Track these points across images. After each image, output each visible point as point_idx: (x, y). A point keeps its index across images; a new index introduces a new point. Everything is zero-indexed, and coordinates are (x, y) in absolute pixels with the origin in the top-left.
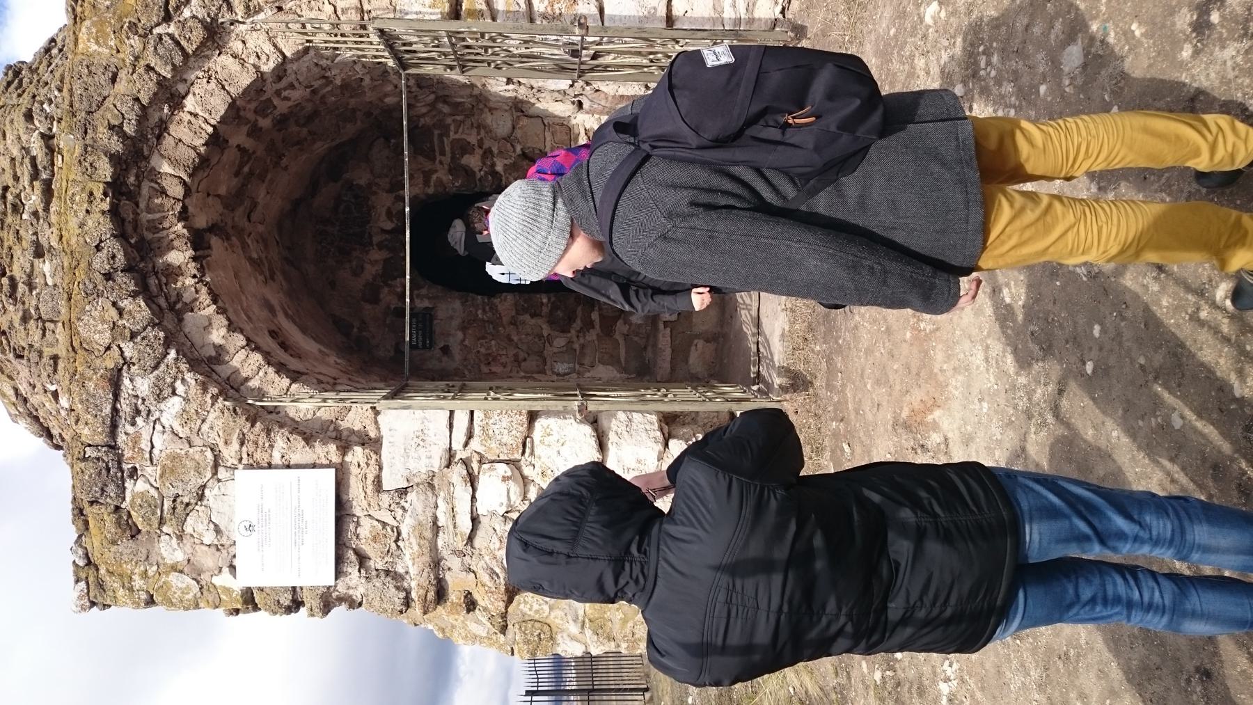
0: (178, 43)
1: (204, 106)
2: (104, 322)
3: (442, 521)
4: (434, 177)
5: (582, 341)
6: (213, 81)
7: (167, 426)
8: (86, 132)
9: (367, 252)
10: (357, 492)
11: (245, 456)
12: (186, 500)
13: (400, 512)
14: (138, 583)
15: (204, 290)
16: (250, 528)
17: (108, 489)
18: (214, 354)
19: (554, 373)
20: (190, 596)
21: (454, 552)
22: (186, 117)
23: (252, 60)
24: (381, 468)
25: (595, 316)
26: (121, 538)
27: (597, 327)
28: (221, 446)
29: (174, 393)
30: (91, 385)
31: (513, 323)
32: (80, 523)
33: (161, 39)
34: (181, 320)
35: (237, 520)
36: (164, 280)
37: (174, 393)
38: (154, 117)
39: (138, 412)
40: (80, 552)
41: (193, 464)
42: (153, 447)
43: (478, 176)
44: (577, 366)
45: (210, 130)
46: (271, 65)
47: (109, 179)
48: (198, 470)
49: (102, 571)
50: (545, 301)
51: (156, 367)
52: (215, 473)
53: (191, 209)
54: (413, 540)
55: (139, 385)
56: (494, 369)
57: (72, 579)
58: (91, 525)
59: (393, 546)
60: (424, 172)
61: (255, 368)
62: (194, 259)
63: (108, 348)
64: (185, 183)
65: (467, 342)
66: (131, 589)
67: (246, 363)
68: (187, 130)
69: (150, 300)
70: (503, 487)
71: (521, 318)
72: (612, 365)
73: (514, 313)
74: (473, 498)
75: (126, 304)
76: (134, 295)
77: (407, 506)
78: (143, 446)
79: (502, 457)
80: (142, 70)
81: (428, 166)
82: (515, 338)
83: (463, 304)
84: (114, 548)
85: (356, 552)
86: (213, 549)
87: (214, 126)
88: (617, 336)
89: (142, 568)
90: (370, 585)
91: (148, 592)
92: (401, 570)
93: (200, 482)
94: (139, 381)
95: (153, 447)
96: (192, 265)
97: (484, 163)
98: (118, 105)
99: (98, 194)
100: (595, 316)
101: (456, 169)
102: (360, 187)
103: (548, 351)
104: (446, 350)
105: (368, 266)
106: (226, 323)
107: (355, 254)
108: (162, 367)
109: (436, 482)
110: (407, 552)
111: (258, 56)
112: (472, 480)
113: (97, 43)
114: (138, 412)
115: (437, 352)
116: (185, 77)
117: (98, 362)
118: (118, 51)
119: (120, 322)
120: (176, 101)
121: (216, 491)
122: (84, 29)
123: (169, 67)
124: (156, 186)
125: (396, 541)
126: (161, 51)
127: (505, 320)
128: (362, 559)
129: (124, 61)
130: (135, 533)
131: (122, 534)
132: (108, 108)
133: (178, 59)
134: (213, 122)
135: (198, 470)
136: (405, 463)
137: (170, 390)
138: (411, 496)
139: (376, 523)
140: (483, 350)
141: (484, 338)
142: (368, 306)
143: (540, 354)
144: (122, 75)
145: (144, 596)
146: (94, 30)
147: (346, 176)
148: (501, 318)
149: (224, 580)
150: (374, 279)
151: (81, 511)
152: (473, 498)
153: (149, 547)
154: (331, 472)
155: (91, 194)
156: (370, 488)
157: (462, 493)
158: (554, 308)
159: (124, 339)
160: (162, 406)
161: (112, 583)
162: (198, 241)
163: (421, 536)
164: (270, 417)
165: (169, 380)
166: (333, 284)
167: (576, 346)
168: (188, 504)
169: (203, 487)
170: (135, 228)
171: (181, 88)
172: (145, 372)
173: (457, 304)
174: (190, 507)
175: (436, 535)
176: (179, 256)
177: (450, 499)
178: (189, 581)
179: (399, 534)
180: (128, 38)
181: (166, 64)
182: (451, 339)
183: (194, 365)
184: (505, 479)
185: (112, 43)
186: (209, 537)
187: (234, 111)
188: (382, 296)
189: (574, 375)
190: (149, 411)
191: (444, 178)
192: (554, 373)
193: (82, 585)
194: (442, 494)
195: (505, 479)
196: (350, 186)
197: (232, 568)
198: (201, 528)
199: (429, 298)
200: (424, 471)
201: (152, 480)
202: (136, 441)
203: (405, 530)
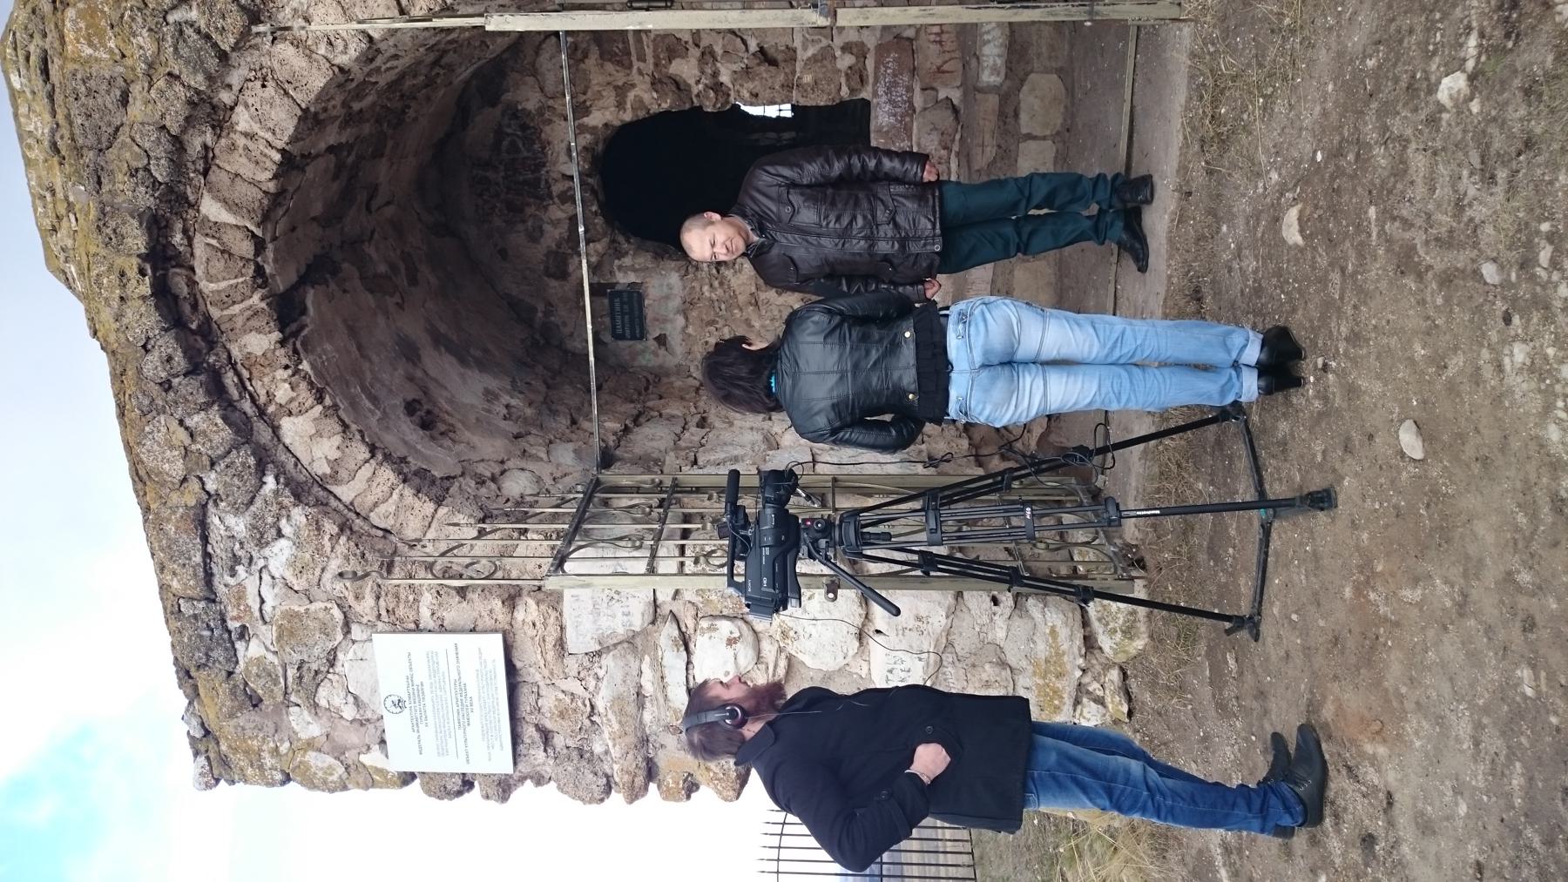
0: (208, 37)
1: (263, 124)
2: (172, 448)
4: (631, 95)
6: (270, 84)
7: (277, 575)
8: (99, 183)
9: (546, 208)
10: (531, 658)
11: (384, 613)
12: (314, 667)
13: (592, 683)
14: (268, 761)
15: (303, 385)
16: (399, 704)
17: (214, 654)
18: (328, 471)
20: (335, 778)
22: (241, 142)
23: (322, 49)
24: (562, 628)
26: (240, 708)
28: (351, 600)
29: (280, 534)
30: (170, 528)
32: (189, 691)
33: (181, 32)
34: (275, 430)
35: (384, 691)
36: (246, 374)
37: (280, 534)
38: (195, 143)
39: (236, 560)
40: (195, 722)
41: (316, 624)
42: (263, 602)
43: (695, 91)
45: (277, 157)
46: (353, 53)
47: (143, 251)
48: (326, 631)
49: (224, 748)
51: (251, 502)
52: (347, 630)
53: (268, 270)
54: (611, 716)
55: (229, 524)
57: (190, 752)
58: (201, 691)
59: (587, 722)
60: (616, 88)
61: (386, 489)
62: (282, 343)
63: (185, 480)
64: (254, 235)
65: (690, 330)
66: (261, 767)
67: (370, 487)
68: (244, 160)
69: (228, 407)
70: (730, 652)
71: (763, 296)
73: (753, 289)
75: (195, 421)
76: (204, 407)
77: (601, 673)
78: (250, 602)
79: (725, 612)
80: (161, 83)
82: (757, 325)
83: (682, 278)
84: (233, 722)
86: (356, 725)
87: (283, 151)
89: (272, 745)
90: (560, 769)
91: (283, 771)
92: (598, 749)
93: (330, 646)
94: (231, 520)
95: (263, 602)
96: (281, 352)
98: (137, 138)
99: (132, 273)
104: (662, 340)
105: (547, 227)
106: (339, 429)
107: (530, 210)
108: (259, 502)
109: (638, 641)
110: (606, 731)
111: (331, 44)
112: (685, 642)
113: (91, 44)
114: (236, 560)
116: (228, 80)
117: (175, 497)
118: (124, 56)
119: (194, 447)
120: (219, 119)
121: (350, 655)
122: (68, 24)
123: (200, 77)
124: (214, 242)
125: (589, 717)
126: (184, 52)
127: (742, 299)
128: (546, 736)
129: (133, 69)
130: (256, 702)
131: (243, 703)
132: (124, 144)
133: (212, 63)
134: (280, 144)
135: (326, 631)
136: (595, 622)
137: (273, 531)
138: (607, 660)
139: (561, 696)
141: (712, 323)
142: (554, 283)
144: (136, 89)
145: (279, 777)
146: (82, 25)
147: (508, 97)
148: (735, 296)
149: (372, 759)
150: (559, 246)
151: (188, 673)
152: (689, 663)
153: (276, 719)
154: (499, 637)
155: (122, 274)
156: (551, 655)
157: (674, 661)
159: (204, 468)
160: (266, 552)
161: (239, 760)
162: (286, 313)
163: (621, 712)
164: (412, 553)
165: (270, 520)
166: (503, 253)
168: (317, 672)
169: (335, 650)
170: (195, 307)
171: (226, 97)
172: (237, 511)
173: (674, 278)
174: (321, 676)
175: (641, 706)
176: (258, 342)
177: (658, 665)
178: (330, 760)
179: (593, 707)
180: (135, 35)
181: (195, 71)
182: (669, 326)
183: (299, 496)
184: (731, 642)
185: (112, 44)
186: (349, 712)
187: (310, 120)
190: (251, 558)
193: (202, 760)
194: (647, 658)
195: (731, 642)
196: (514, 112)
197: (383, 742)
198: (337, 701)
199: (635, 270)
200: (621, 631)
201: (268, 643)
202: (240, 594)
203: (601, 705)
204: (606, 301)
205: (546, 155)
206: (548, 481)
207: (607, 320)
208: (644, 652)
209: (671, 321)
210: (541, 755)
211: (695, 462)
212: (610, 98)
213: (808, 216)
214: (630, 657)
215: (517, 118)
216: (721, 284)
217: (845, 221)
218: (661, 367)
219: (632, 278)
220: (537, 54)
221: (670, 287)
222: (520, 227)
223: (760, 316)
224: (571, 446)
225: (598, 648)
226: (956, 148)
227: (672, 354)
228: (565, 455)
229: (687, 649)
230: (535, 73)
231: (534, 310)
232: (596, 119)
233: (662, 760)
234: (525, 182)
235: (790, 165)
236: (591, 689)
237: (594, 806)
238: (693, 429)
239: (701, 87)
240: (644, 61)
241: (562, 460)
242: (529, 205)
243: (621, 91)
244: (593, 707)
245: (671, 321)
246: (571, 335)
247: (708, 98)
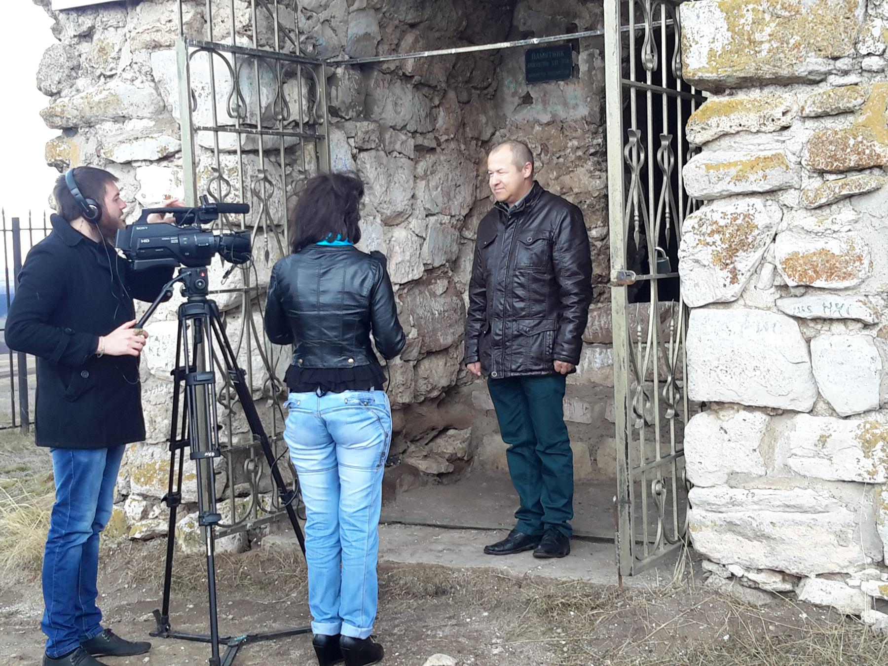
3: (129, 126)
13: (128, 75)
21: (100, 145)
54: (105, 93)
59: (98, 73)
65: (537, 128)
74: (151, 162)
77: (137, 83)
85: (92, 29)
104: (527, 100)
109: (166, 115)
115: (524, 89)
128: (87, 36)
152: (151, 162)
157: (149, 149)
177: (147, 135)
179: (111, 76)
203: (112, 83)
206: (323, 16)
208: (157, 121)
210: (72, 33)
211: (361, 150)
213: (524, 258)
214: (151, 109)
217: (520, 292)
218: (503, 100)
224: (374, 29)
225: (156, 80)
228: (362, 25)
229: (160, 160)
233: (78, 140)
235: (571, 240)
236: (124, 75)
237: (35, 83)
238: (411, 142)
241: (352, 25)
244: (111, 76)
245: (545, 109)
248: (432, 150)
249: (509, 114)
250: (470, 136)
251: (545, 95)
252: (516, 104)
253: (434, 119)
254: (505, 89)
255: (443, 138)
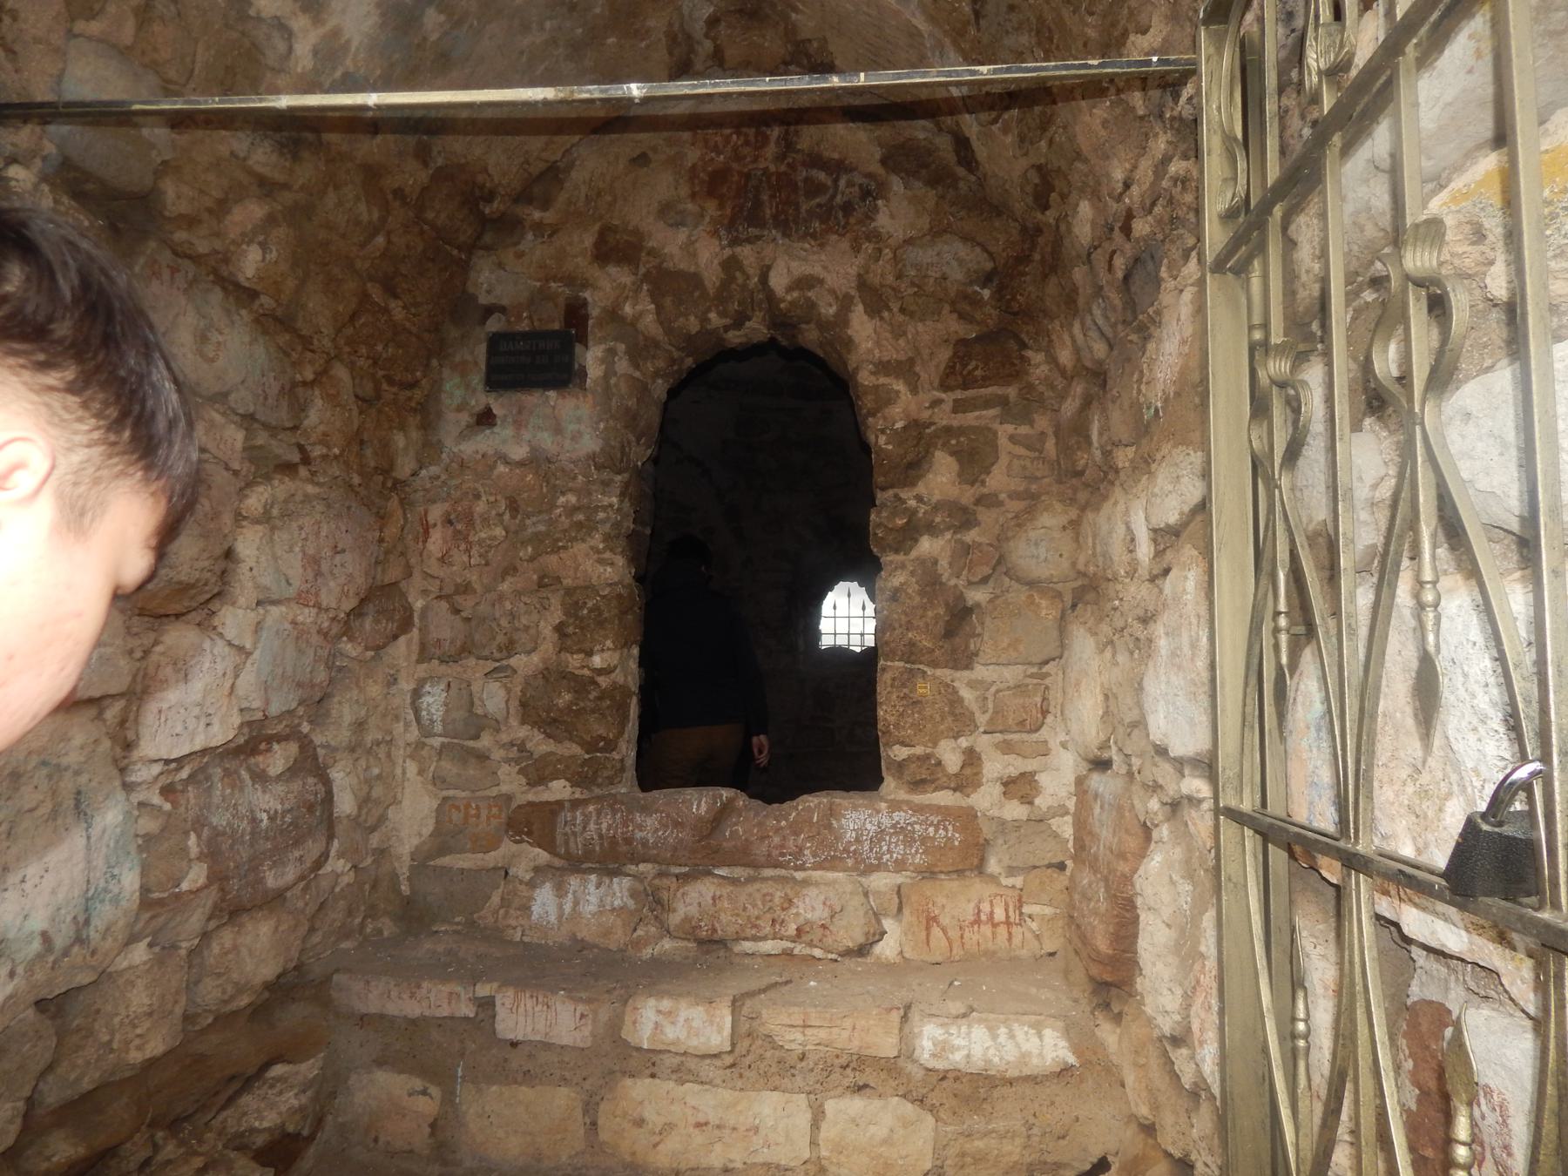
4: (899, 386)
5: (498, 754)
9: (715, 233)
19: (421, 682)
25: (559, 790)
27: (531, 797)
31: (546, 582)
43: (905, 494)
44: (436, 742)
50: (597, 661)
56: (436, 536)
60: (911, 361)
71: (555, 601)
72: (436, 833)
73: (567, 582)
81: (929, 373)
82: (505, 587)
83: (592, 457)
88: (507, 847)
97: (936, 508)
100: (559, 790)
101: (920, 442)
102: (870, 216)
103: (474, 668)
104: (485, 419)
105: (682, 235)
107: (711, 207)
115: (481, 399)
140: (480, 507)
141: (514, 507)
142: (589, 240)
143: (466, 649)
147: (896, 184)
150: (652, 252)
158: (580, 685)
167: (485, 741)
173: (590, 443)
188: (613, 270)
189: (414, 734)
191: (896, 410)
192: (421, 682)
196: (871, 193)
199: (606, 376)
204: (556, 326)
205: (803, 238)
207: (524, 326)
209: (518, 438)
212: (894, 351)
215: (863, 199)
216: (579, 525)
218: (439, 415)
219: (594, 371)
220: (966, 238)
221: (576, 437)
222: (684, 191)
223: (518, 594)
226: (799, 949)
227: (462, 437)
230: (937, 232)
231: (545, 204)
232: (863, 329)
234: (758, 204)
239: (912, 503)
240: (955, 411)
242: (721, 207)
243: (905, 369)
246: (500, 266)
247: (894, 514)
248: (288, 469)
249: (449, 442)
250: (372, 464)
251: (520, 412)
252: (464, 424)
253: (300, 409)
254: (443, 396)
255: (317, 451)
